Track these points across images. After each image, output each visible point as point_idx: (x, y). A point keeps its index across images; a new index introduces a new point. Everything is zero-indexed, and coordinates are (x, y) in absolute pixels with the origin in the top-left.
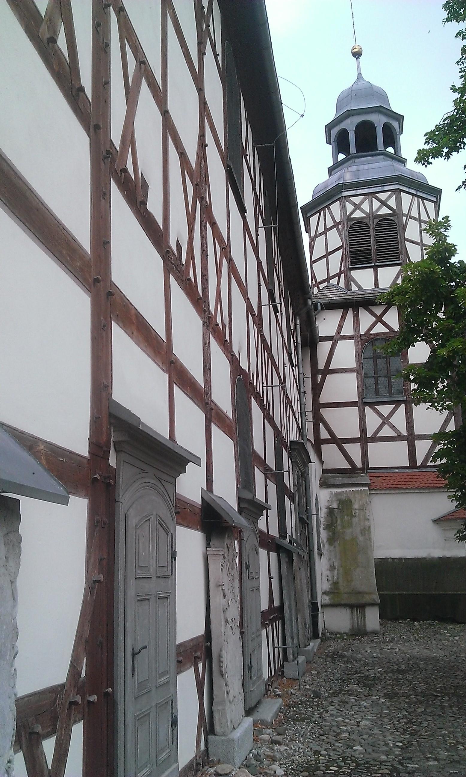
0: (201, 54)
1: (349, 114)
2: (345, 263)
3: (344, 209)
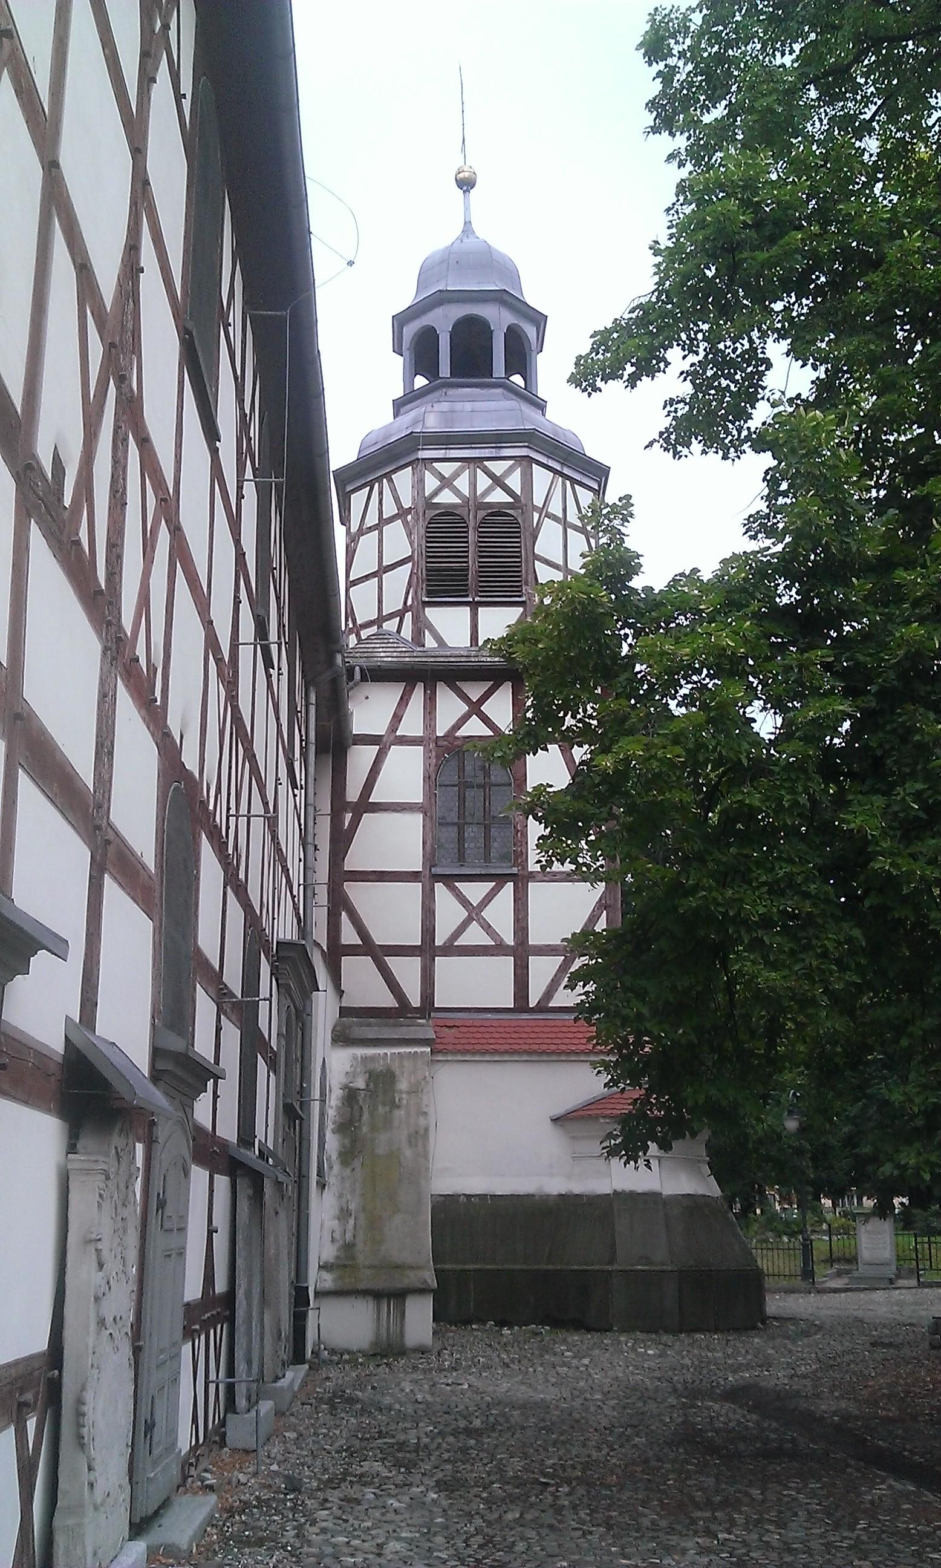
0: (147, 79)
1: (442, 298)
2: (416, 592)
3: (419, 484)
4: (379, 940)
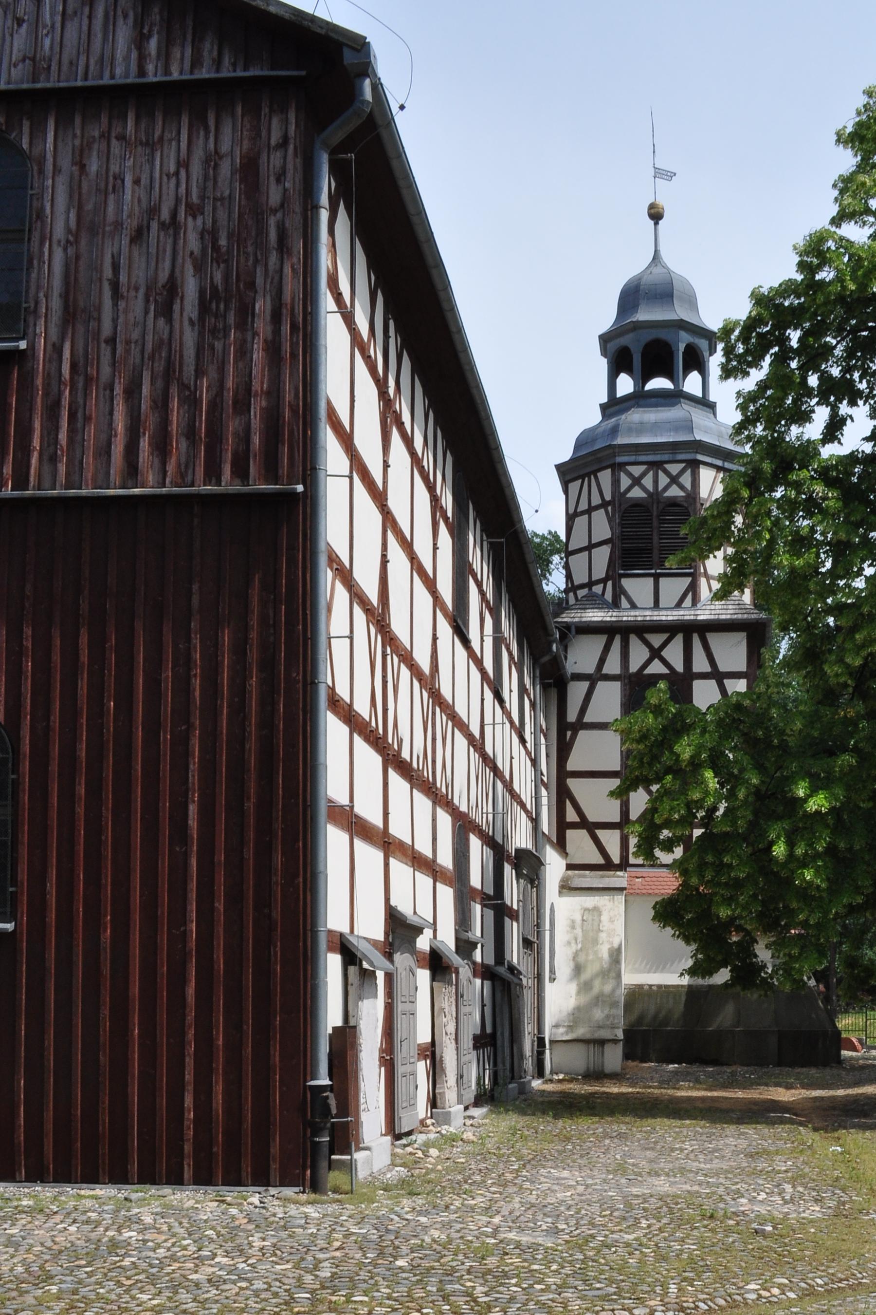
3: (616, 482)
4: (592, 818)
